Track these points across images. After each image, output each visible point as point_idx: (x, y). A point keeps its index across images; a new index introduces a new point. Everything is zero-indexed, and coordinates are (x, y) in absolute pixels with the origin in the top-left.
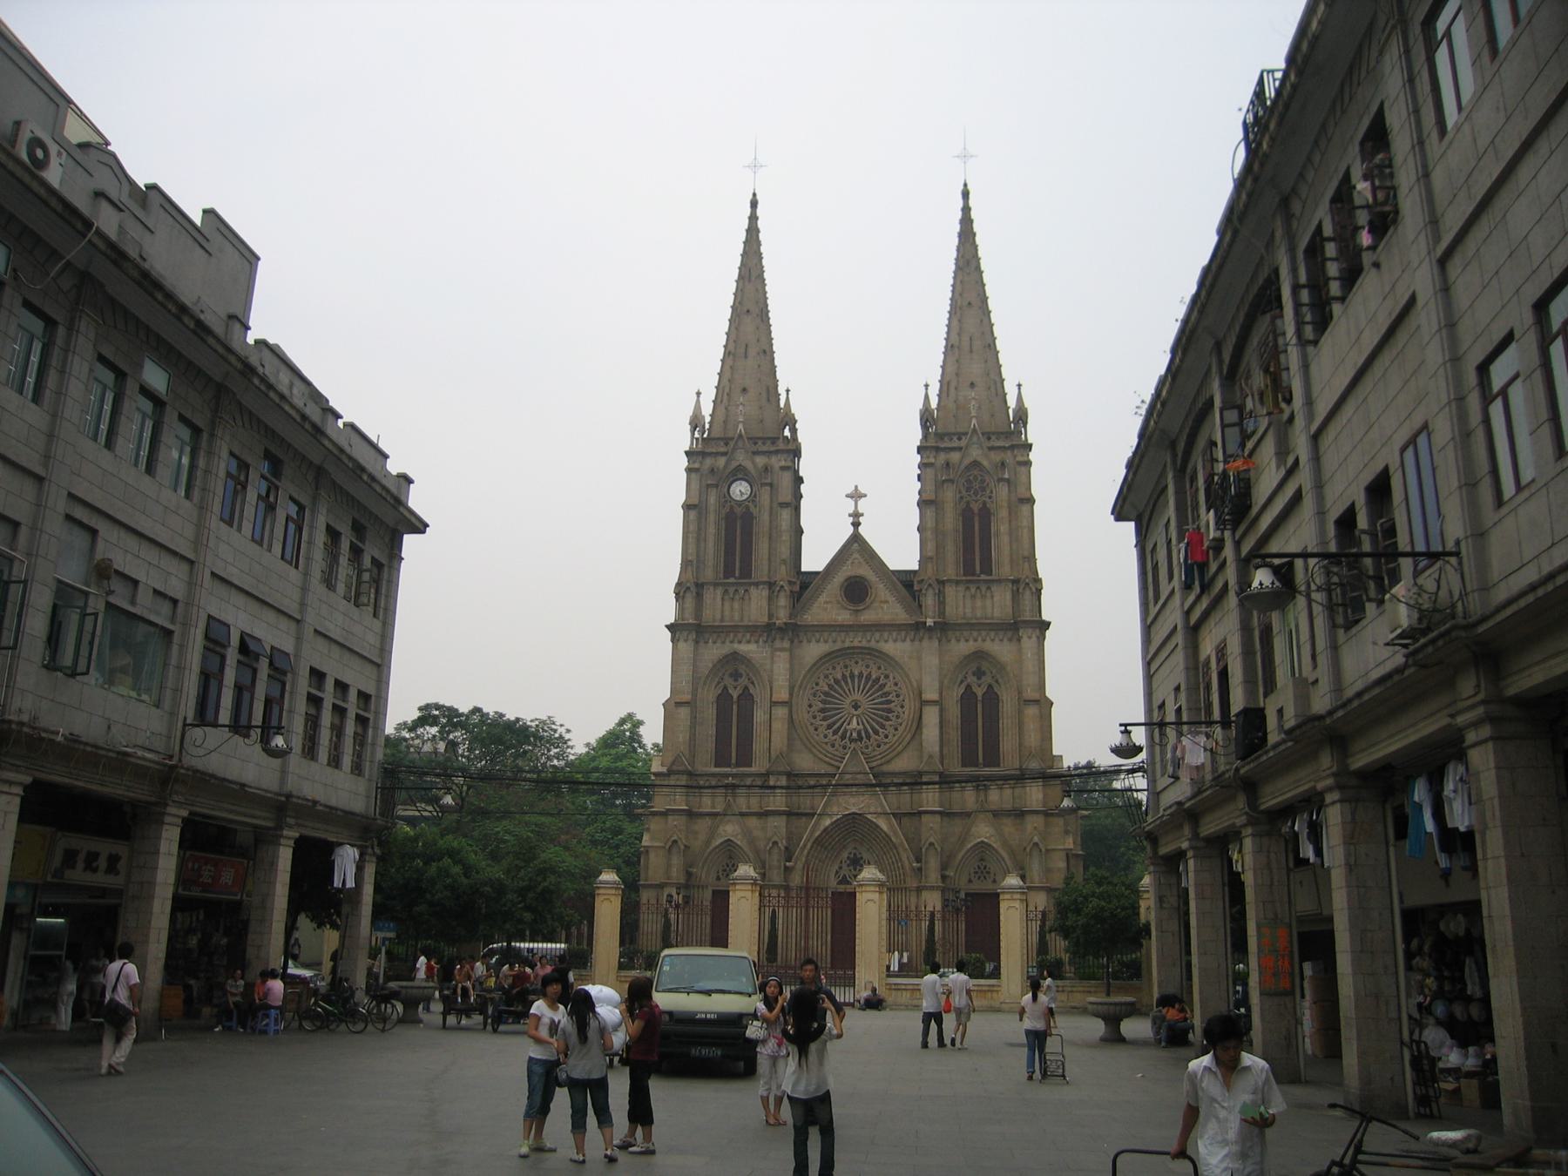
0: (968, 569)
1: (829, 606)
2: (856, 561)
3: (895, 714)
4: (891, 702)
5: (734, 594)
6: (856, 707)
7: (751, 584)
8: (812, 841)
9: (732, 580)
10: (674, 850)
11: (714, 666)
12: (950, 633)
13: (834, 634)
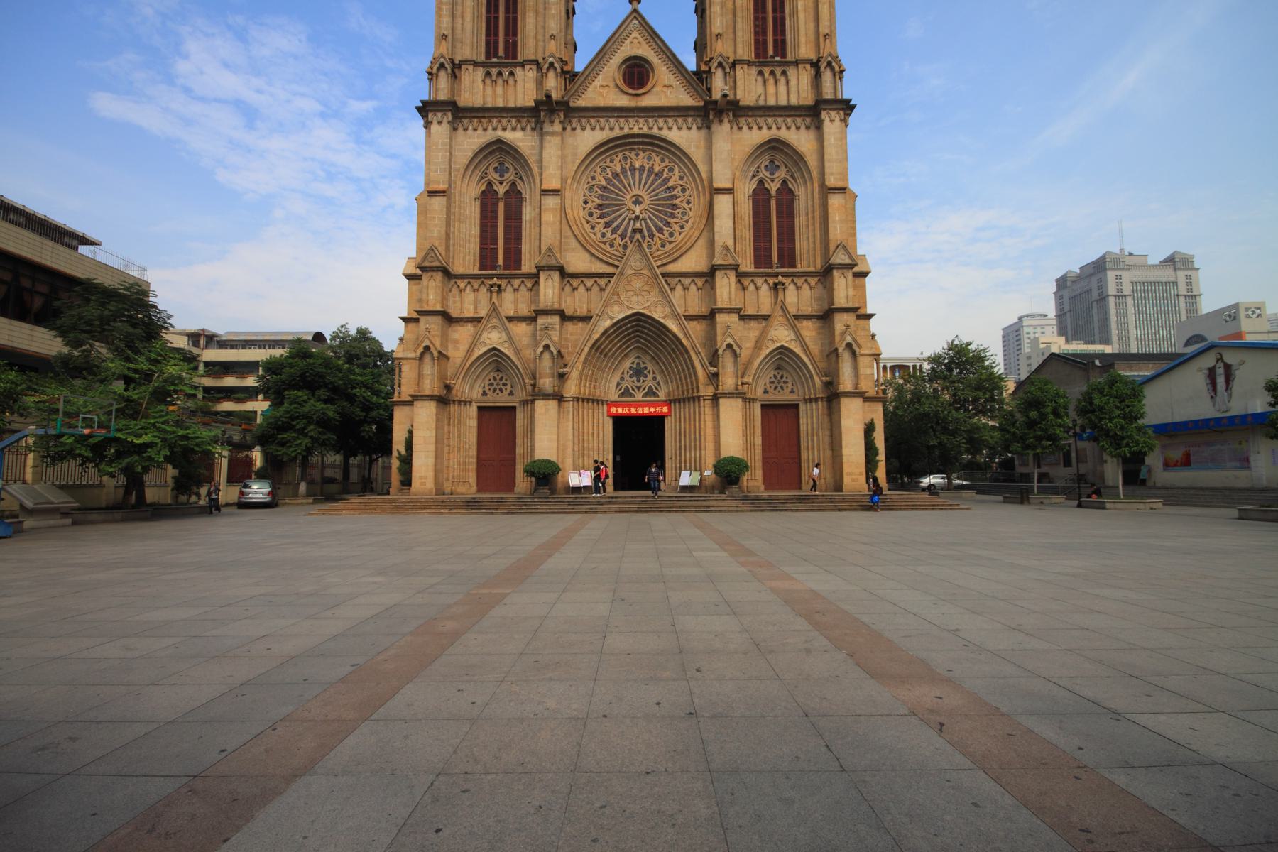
0: (760, 46)
1: (605, 91)
2: (635, 41)
3: (681, 210)
4: (677, 197)
5: (497, 77)
6: (635, 203)
7: (516, 65)
8: (589, 344)
9: (495, 60)
10: (427, 359)
11: (476, 155)
12: (742, 121)
13: (612, 120)
